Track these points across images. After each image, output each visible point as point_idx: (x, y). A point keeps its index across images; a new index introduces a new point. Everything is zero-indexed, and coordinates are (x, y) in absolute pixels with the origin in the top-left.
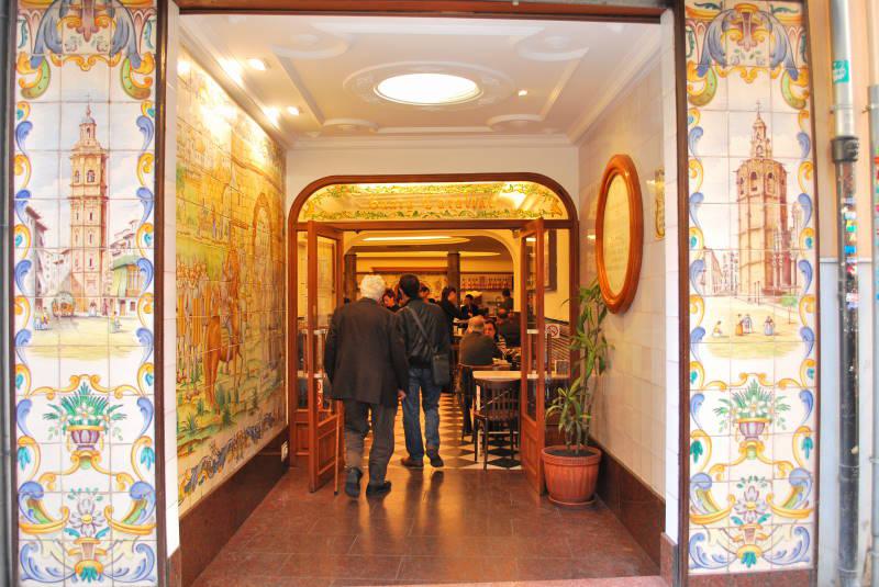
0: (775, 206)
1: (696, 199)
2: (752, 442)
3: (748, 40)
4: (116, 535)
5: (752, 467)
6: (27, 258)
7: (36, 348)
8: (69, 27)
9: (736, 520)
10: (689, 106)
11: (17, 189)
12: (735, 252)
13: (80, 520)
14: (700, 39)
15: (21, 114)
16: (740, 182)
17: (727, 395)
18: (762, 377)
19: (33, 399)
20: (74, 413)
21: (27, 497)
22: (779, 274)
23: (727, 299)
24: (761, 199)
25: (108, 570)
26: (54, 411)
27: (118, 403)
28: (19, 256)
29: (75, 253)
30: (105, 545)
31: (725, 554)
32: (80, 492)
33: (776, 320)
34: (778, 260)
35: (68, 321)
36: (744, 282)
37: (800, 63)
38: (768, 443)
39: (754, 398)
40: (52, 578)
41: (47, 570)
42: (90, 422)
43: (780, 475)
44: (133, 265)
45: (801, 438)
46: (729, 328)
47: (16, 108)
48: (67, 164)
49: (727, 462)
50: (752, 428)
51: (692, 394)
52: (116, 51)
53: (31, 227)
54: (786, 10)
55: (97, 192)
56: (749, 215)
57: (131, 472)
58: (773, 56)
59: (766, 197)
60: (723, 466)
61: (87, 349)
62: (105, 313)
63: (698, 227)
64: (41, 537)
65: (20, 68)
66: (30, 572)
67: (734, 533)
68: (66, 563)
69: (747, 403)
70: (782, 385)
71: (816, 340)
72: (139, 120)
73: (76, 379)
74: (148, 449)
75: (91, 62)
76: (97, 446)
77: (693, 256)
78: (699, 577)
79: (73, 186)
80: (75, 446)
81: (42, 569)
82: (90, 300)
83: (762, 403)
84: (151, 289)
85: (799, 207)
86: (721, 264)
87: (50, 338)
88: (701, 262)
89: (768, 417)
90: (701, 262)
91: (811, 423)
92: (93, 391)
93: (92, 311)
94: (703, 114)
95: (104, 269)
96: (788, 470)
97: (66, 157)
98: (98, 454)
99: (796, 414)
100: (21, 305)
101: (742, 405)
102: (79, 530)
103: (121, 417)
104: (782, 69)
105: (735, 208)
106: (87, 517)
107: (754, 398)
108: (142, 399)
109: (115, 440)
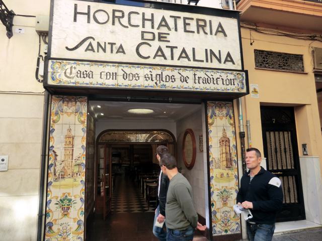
0: (228, 148)
2: (225, 204)
3: (221, 110)
7: (54, 186)
9: (222, 222)
11: (50, 146)
14: (211, 111)
15: (52, 127)
16: (220, 142)
18: (226, 187)
22: (229, 163)
37: (232, 115)
38: (229, 203)
46: (219, 176)
49: (219, 207)
57: (77, 217)
61: (67, 186)
65: (52, 115)
67: (222, 225)
70: (231, 189)
75: (70, 115)
77: (210, 160)
87: (57, 183)
88: (212, 161)
90: (212, 161)
100: (50, 175)
103: (75, 203)
106: (65, 231)
108: (81, 199)
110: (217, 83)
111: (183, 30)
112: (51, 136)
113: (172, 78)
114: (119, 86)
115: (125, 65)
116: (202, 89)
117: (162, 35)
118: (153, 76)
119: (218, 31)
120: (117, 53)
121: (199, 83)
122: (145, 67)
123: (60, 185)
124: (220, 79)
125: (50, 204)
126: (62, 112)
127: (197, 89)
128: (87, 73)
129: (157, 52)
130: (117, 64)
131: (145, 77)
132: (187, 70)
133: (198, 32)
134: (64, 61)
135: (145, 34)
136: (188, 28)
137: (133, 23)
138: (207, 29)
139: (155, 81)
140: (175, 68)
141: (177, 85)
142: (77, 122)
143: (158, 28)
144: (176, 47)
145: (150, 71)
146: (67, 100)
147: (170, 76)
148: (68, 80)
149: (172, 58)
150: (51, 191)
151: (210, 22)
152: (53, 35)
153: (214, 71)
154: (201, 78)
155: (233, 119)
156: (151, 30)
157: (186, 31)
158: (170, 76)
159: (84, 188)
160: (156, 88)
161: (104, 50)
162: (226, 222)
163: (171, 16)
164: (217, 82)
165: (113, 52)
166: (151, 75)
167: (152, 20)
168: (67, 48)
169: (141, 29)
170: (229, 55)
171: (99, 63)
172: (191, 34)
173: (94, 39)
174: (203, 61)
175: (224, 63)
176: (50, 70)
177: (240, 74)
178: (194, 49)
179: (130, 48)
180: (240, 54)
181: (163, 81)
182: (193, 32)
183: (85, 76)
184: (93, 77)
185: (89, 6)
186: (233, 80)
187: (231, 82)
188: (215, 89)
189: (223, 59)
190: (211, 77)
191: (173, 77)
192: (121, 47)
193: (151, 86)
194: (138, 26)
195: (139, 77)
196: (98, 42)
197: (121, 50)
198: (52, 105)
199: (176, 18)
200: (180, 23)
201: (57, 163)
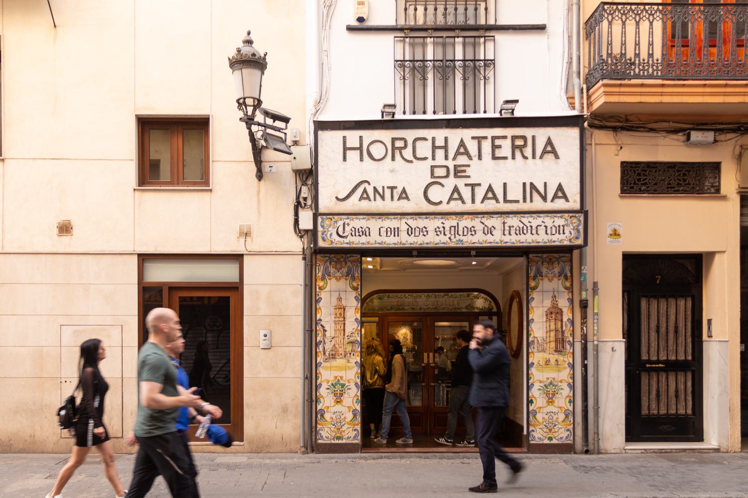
0: (559, 324)
1: (531, 321)
2: (550, 401)
3: (551, 268)
5: (551, 408)
7: (324, 367)
8: (333, 268)
9: (545, 426)
10: (530, 290)
11: (318, 319)
14: (534, 268)
15: (318, 295)
16: (547, 315)
17: (542, 385)
18: (554, 379)
20: (335, 388)
22: (560, 345)
23: (542, 353)
24: (554, 321)
25: (344, 437)
26: (329, 387)
28: (318, 339)
31: (542, 437)
32: (336, 412)
34: (560, 341)
35: (333, 359)
37: (569, 274)
38: (556, 401)
39: (551, 386)
43: (561, 411)
45: (568, 399)
48: (333, 311)
49: (541, 406)
50: (551, 396)
51: (530, 384)
52: (348, 275)
53: (322, 330)
56: (550, 326)
57: (353, 406)
59: (555, 319)
60: (541, 408)
61: (339, 368)
62: (345, 357)
63: (532, 330)
69: (549, 387)
70: (561, 382)
71: (572, 366)
72: (355, 297)
73: (336, 377)
74: (358, 399)
75: (340, 279)
76: (342, 398)
78: (533, 444)
82: (340, 353)
83: (554, 387)
84: (359, 349)
85: (567, 323)
86: (540, 342)
87: (328, 364)
88: (533, 341)
89: (556, 392)
90: (533, 341)
91: (571, 394)
96: (564, 410)
99: (566, 391)
101: (548, 388)
103: (349, 389)
104: (562, 277)
105: (545, 323)
106: (338, 420)
107: (551, 386)
108: (356, 384)
110: (537, 233)
111: (490, 156)
112: (318, 307)
113: (472, 231)
114: (403, 244)
115: (409, 217)
116: (513, 243)
117: (459, 169)
118: (446, 229)
120: (399, 200)
121: (510, 234)
122: (435, 218)
124: (543, 227)
125: (321, 389)
126: (330, 276)
127: (506, 242)
128: (363, 230)
130: (399, 216)
131: (436, 232)
132: (492, 217)
134: (336, 217)
135: (436, 170)
136: (498, 153)
137: (419, 154)
139: (449, 235)
140: (476, 216)
143: (454, 159)
144: (479, 185)
145: (442, 223)
146: (335, 259)
147: (469, 227)
148: (341, 239)
149: (473, 201)
152: (319, 182)
154: (513, 227)
155: (569, 280)
157: (494, 158)
158: (469, 227)
160: (450, 245)
161: (383, 197)
162: (550, 427)
166: (444, 228)
167: (445, 148)
168: (337, 198)
169: (430, 162)
171: (378, 217)
173: (369, 184)
174: (517, 201)
177: (575, 217)
178: (505, 184)
179: (416, 194)
180: (579, 184)
181: (460, 235)
182: (505, 158)
183: (361, 234)
184: (371, 235)
185: (361, 137)
186: (563, 226)
187: (559, 230)
188: (533, 242)
189: (550, 196)
190: (528, 225)
192: (404, 191)
193: (444, 243)
194: (425, 159)
195: (427, 232)
196: (374, 188)
197: (404, 195)
198: (317, 267)
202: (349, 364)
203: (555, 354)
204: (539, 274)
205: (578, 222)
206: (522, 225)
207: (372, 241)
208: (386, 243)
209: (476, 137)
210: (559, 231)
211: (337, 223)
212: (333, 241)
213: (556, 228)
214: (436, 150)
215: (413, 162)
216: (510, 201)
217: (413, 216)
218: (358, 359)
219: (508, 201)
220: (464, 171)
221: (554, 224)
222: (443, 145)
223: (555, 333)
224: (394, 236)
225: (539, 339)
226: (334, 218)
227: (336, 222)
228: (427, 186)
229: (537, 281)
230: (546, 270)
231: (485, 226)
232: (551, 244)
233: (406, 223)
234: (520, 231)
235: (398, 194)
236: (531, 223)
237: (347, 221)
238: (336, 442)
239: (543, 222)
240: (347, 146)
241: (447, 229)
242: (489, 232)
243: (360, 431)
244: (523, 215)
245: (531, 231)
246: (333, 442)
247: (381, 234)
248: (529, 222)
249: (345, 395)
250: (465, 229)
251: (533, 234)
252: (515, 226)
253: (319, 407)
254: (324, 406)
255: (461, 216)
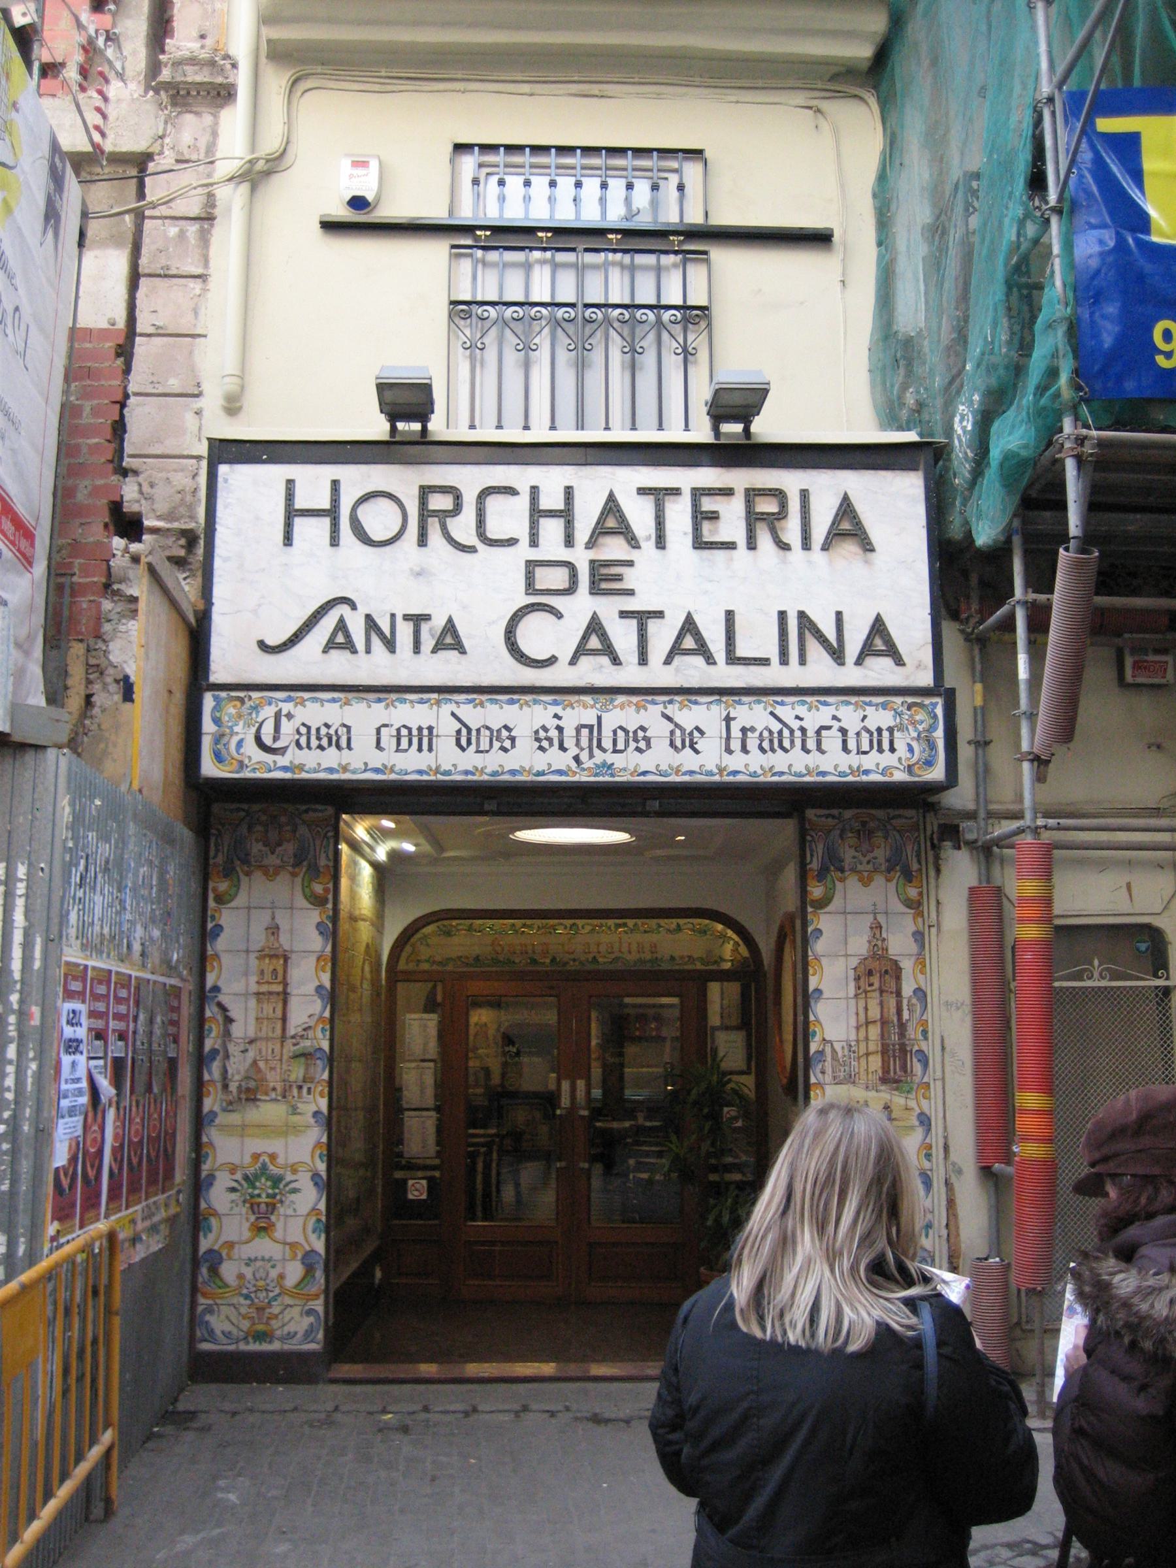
0: (892, 1002)
1: (816, 995)
4: (288, 1300)
6: (216, 1047)
7: (222, 1128)
8: (257, 841)
10: (810, 909)
12: (853, 1044)
13: (255, 1286)
14: (820, 848)
15: (213, 918)
16: (857, 979)
19: (217, 1174)
20: (254, 1188)
21: (207, 1264)
24: (877, 994)
25: (278, 1333)
27: (293, 1178)
28: (208, 1044)
29: (258, 1043)
30: (276, 1310)
33: (893, 1107)
34: (894, 1051)
35: (250, 1104)
36: (862, 1070)
40: (225, 1341)
41: (223, 1333)
42: (268, 1196)
44: (310, 1054)
47: (209, 913)
48: (253, 962)
53: (220, 1018)
54: (900, 816)
55: (280, 988)
56: (866, 1009)
57: (303, 1241)
58: (888, 861)
59: (882, 992)
61: (266, 1130)
62: (284, 1097)
63: (818, 1021)
64: (219, 1301)
66: (206, 1335)
68: (241, 1326)
72: (319, 925)
73: (256, 1156)
75: (276, 873)
76: (273, 1218)
79: (258, 983)
80: (252, 1218)
81: (218, 1332)
82: (272, 1084)
84: (326, 1076)
85: (914, 1001)
86: (840, 1054)
87: (234, 1118)
88: (821, 1053)
90: (821, 1053)
92: (272, 1167)
93: (273, 1095)
94: (822, 917)
95: (285, 1057)
97: (253, 956)
98: (274, 1225)
102: (253, 1295)
103: (295, 1191)
105: (853, 1002)
106: (261, 1283)
108: (315, 1176)
109: (290, 1212)
110: (819, 749)
111: (689, 540)
112: (210, 952)
113: (640, 739)
114: (444, 774)
117: (604, 571)
119: (835, 535)
120: (434, 651)
121: (744, 749)
122: (535, 702)
123: (244, 1126)
124: (834, 732)
127: (735, 773)
128: (332, 731)
129: (585, 638)
130: (435, 696)
131: (538, 740)
132: (696, 703)
133: (752, 545)
134: (255, 695)
135: (540, 572)
137: (493, 532)
138: (792, 530)
139: (573, 751)
140: (650, 698)
141: (657, 763)
142: (301, 902)
143: (591, 544)
144: (659, 614)
145: (556, 716)
146: (264, 818)
147: (631, 729)
148: (269, 758)
149: (643, 660)
150: (211, 1144)
151: (804, 495)
152: (214, 600)
153: (809, 699)
154: (753, 729)
156: (564, 554)
157: (699, 544)
158: (631, 729)
159: (324, 1139)
160: (576, 778)
161: (390, 644)
163: (642, 491)
164: (819, 743)
165: (423, 648)
166: (560, 729)
167: (566, 514)
168: (262, 645)
169: (524, 552)
170: (878, 627)
172: (720, 555)
173: (353, 606)
174: (764, 662)
175: (859, 662)
176: (208, 726)
177: (921, 706)
179: (483, 632)
181: (604, 751)
182: (730, 546)
183: (325, 742)
184: (353, 745)
185: (335, 484)
186: (891, 730)
187: (879, 740)
188: (809, 773)
189: (853, 648)
190: (795, 725)
191: (641, 734)
193: (560, 772)
194: (511, 542)
195: (513, 739)
196: (368, 617)
199: (660, 495)
200: (679, 514)
201: (232, 1048)
202: (295, 1118)
203: (883, 1088)
204: (833, 865)
205: (932, 721)
206: (780, 726)
207: (358, 764)
208: (396, 769)
209: (650, 489)
210: (880, 743)
211: (258, 713)
212: (246, 761)
213: (871, 734)
214: (542, 521)
215: (476, 551)
216: (745, 659)
217: (475, 696)
218: (323, 1104)
219: (739, 659)
220: (619, 578)
221: (867, 723)
222: (561, 506)
223: (882, 1028)
224: (420, 750)
225: (837, 1047)
226: (250, 698)
227: (256, 708)
228: (515, 615)
229: (830, 885)
230: (852, 852)
231: (677, 725)
232: (858, 779)
233: (453, 714)
234: (771, 741)
235: (433, 636)
236: (801, 719)
237: (286, 707)
238: (254, 1347)
239: (835, 718)
240: (297, 506)
241: (569, 732)
242: (687, 744)
243: (322, 1314)
244: (779, 699)
245: (804, 742)
246: (243, 1347)
247: (382, 745)
248: (797, 717)
249: (281, 1210)
250: (620, 733)
251: (808, 752)
252: (760, 728)
253: (205, 1244)
254: (220, 1242)
255: (608, 697)
